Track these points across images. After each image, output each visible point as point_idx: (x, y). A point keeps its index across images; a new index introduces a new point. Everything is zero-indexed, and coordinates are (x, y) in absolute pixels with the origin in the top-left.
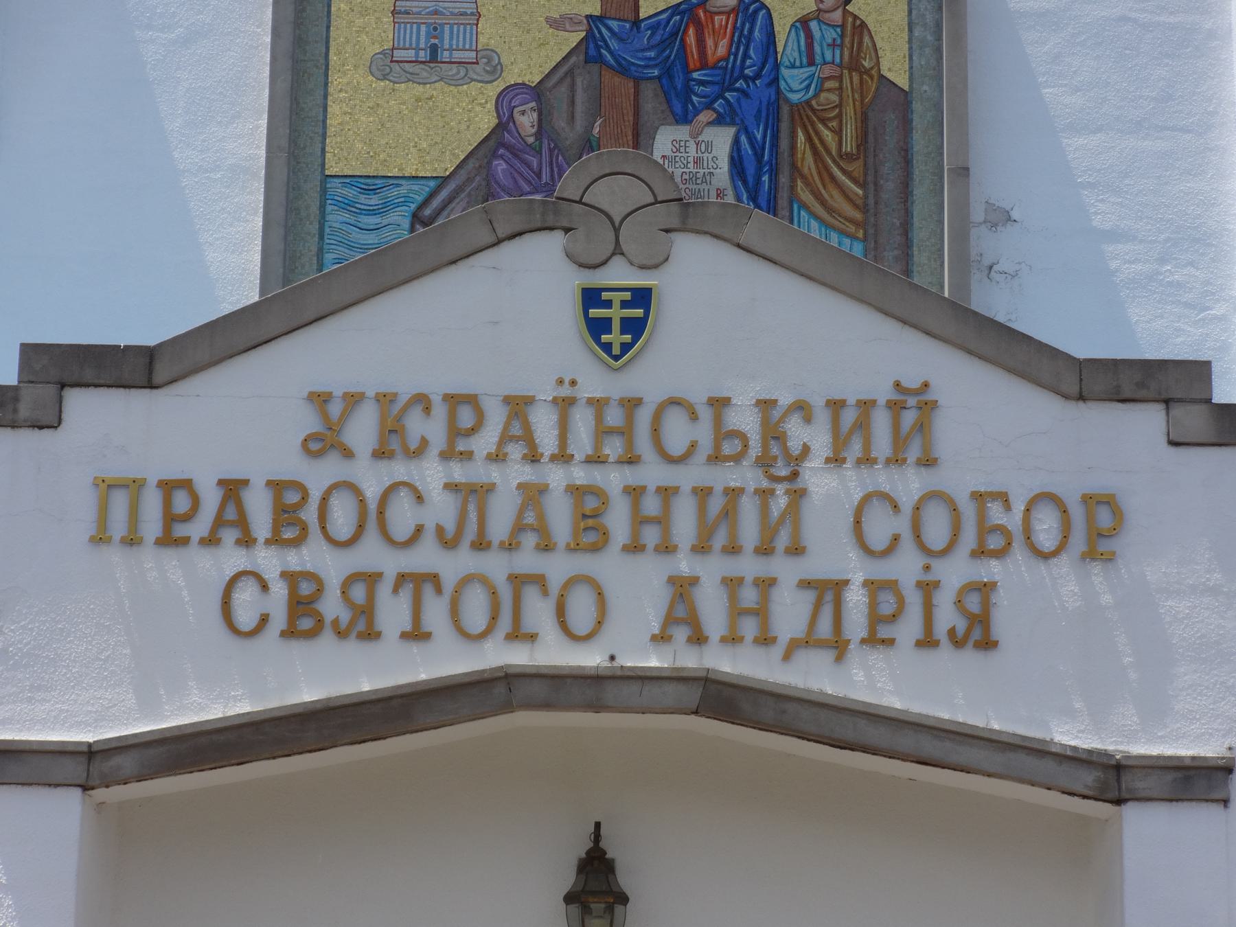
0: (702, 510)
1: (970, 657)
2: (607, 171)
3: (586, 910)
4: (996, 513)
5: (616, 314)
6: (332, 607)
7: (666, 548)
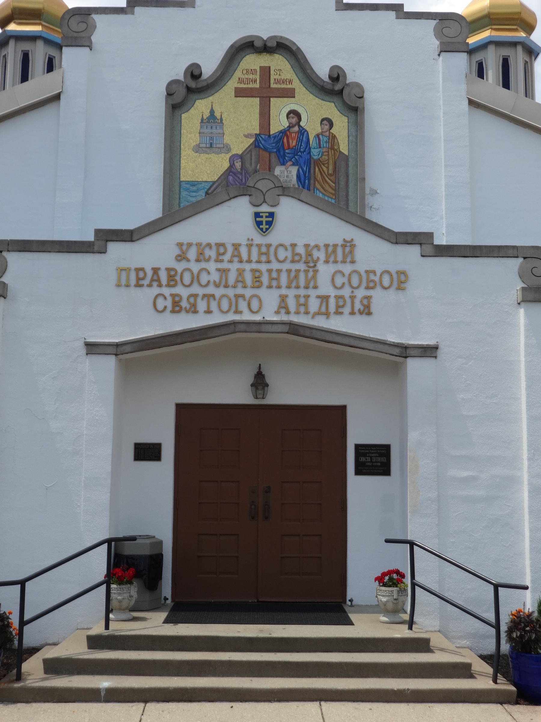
0: (289, 276)
1: (364, 318)
2: (261, 178)
3: (257, 389)
4: (372, 277)
5: (264, 220)
6: (184, 304)
7: (279, 287)
